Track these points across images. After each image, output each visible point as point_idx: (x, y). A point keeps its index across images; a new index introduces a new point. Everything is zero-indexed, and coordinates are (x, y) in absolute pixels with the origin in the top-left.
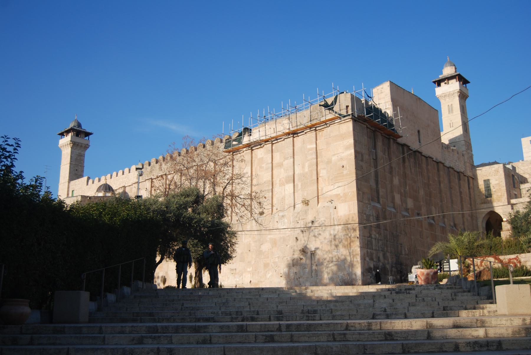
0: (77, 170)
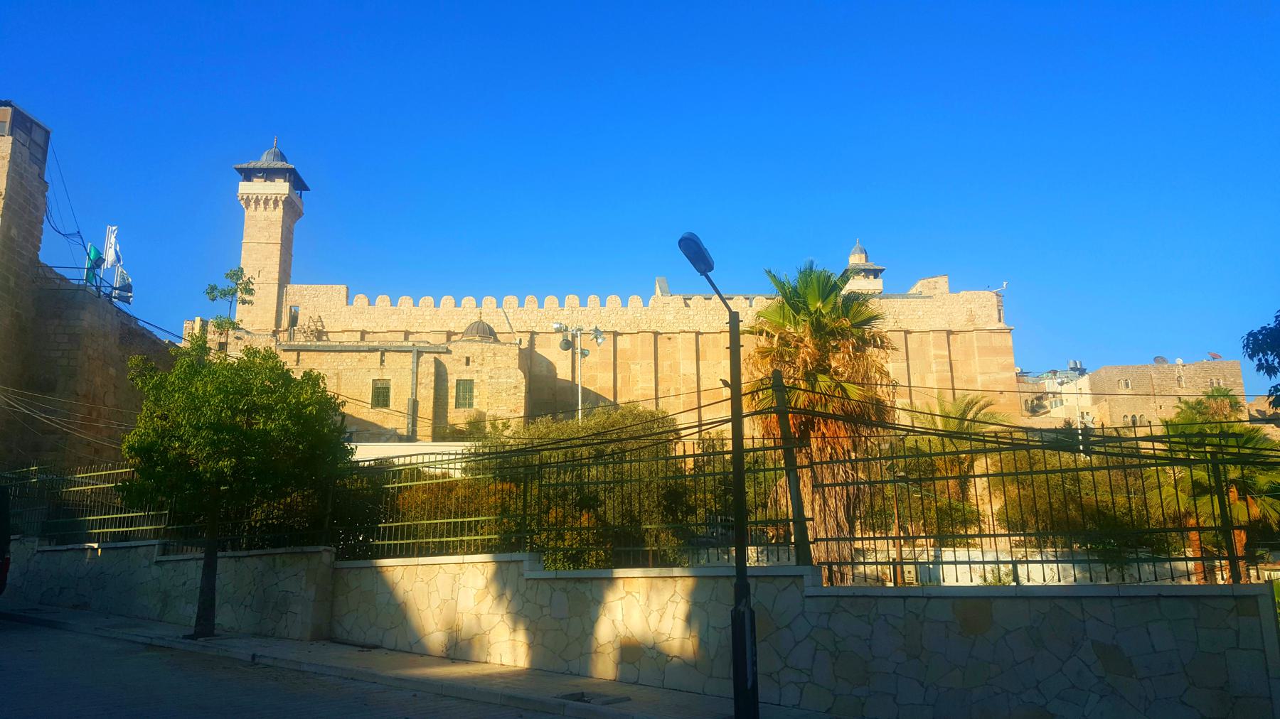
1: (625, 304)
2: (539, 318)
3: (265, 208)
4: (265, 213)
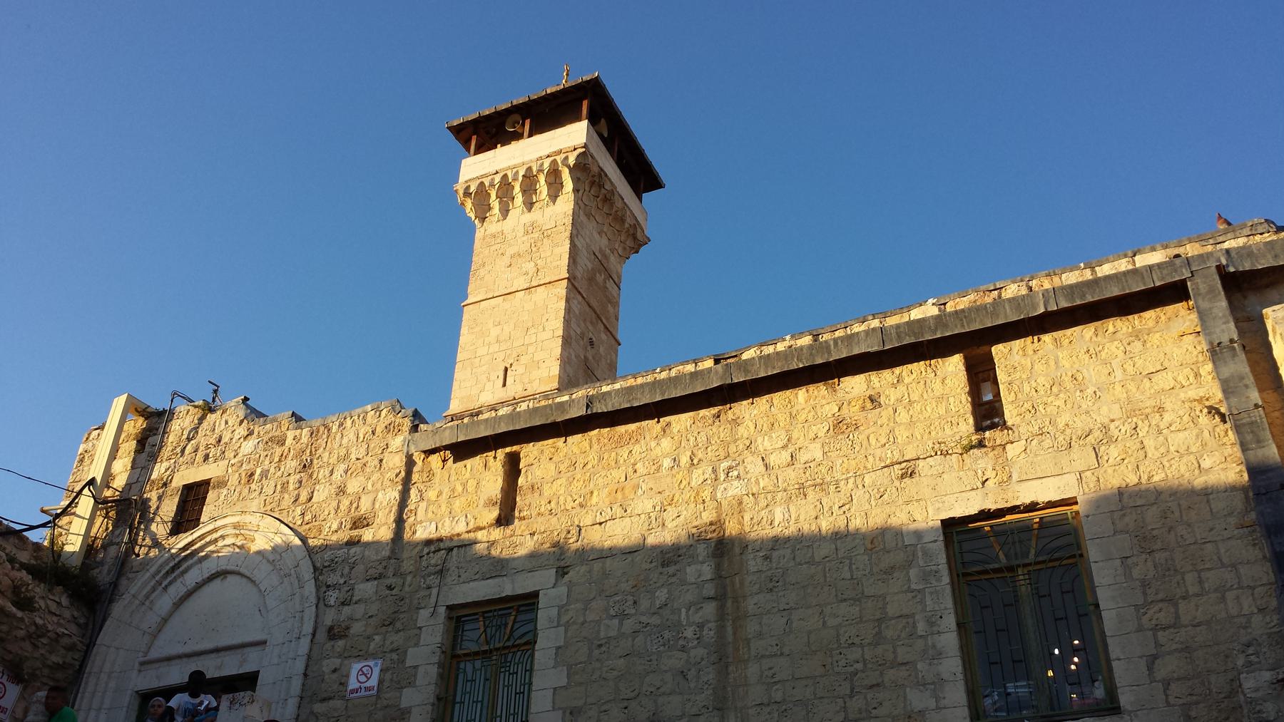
3: (529, 205)
4: (528, 217)
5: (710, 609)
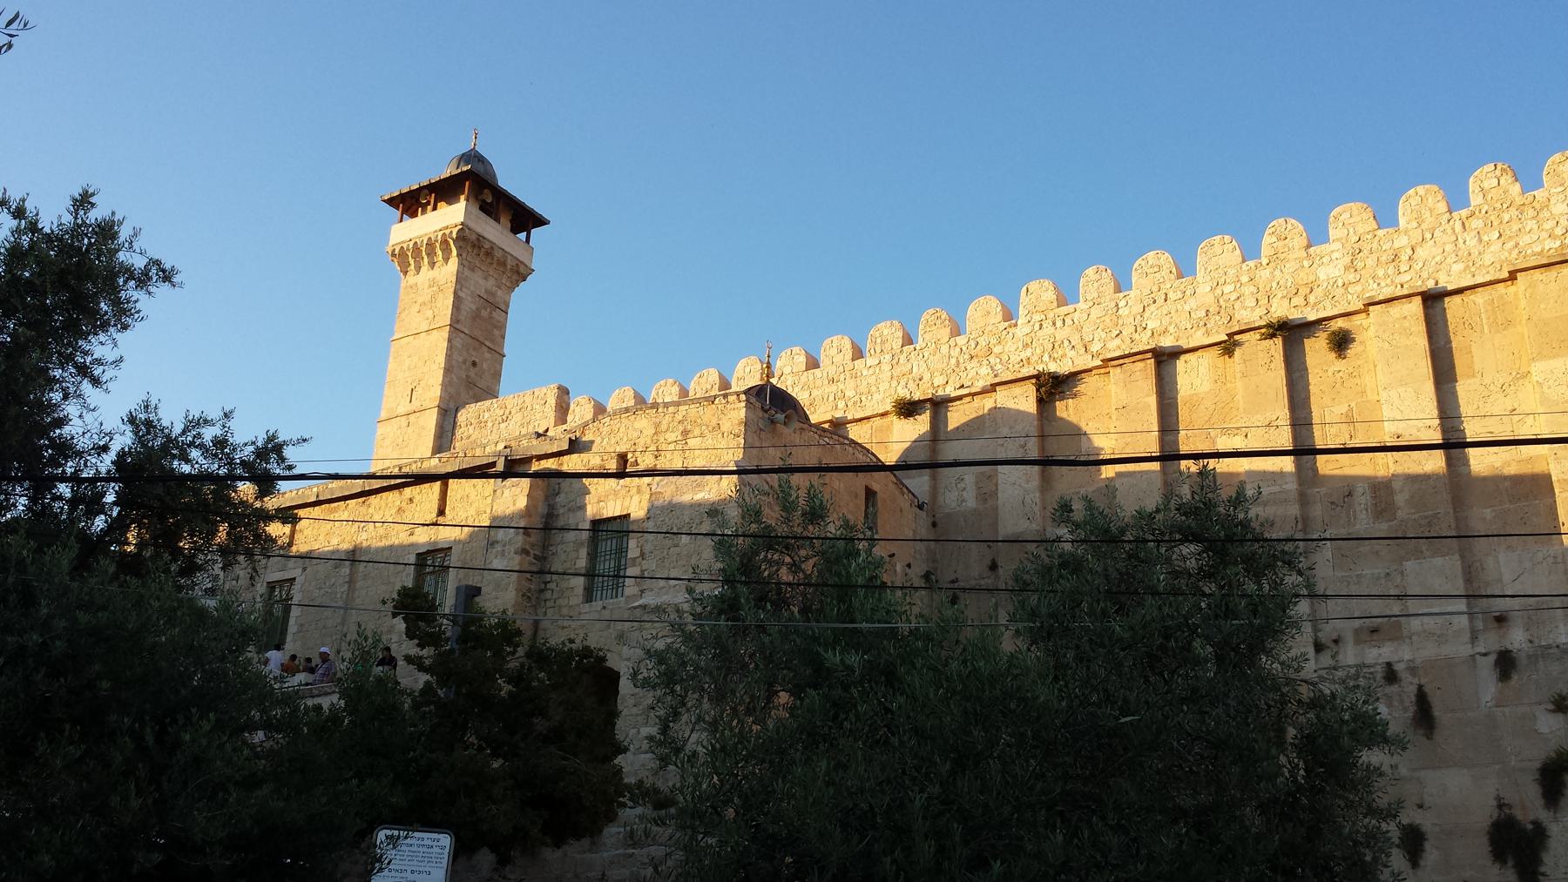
0: (474, 364)
1: (1184, 269)
2: (953, 361)
5: (346, 586)
